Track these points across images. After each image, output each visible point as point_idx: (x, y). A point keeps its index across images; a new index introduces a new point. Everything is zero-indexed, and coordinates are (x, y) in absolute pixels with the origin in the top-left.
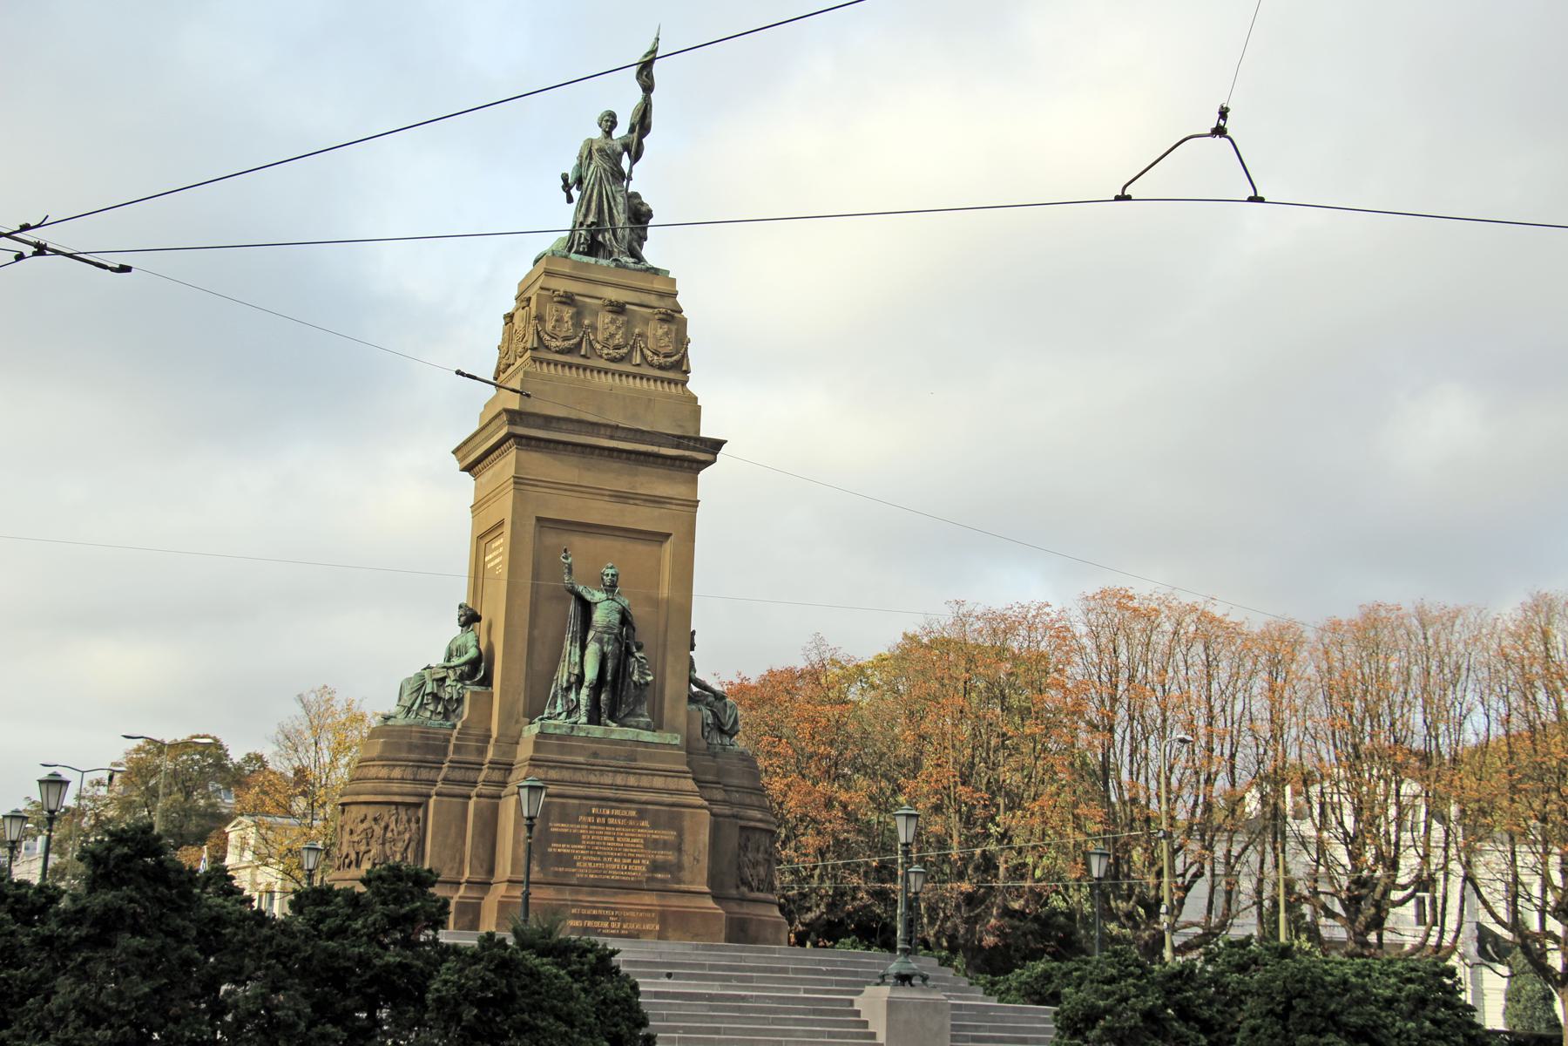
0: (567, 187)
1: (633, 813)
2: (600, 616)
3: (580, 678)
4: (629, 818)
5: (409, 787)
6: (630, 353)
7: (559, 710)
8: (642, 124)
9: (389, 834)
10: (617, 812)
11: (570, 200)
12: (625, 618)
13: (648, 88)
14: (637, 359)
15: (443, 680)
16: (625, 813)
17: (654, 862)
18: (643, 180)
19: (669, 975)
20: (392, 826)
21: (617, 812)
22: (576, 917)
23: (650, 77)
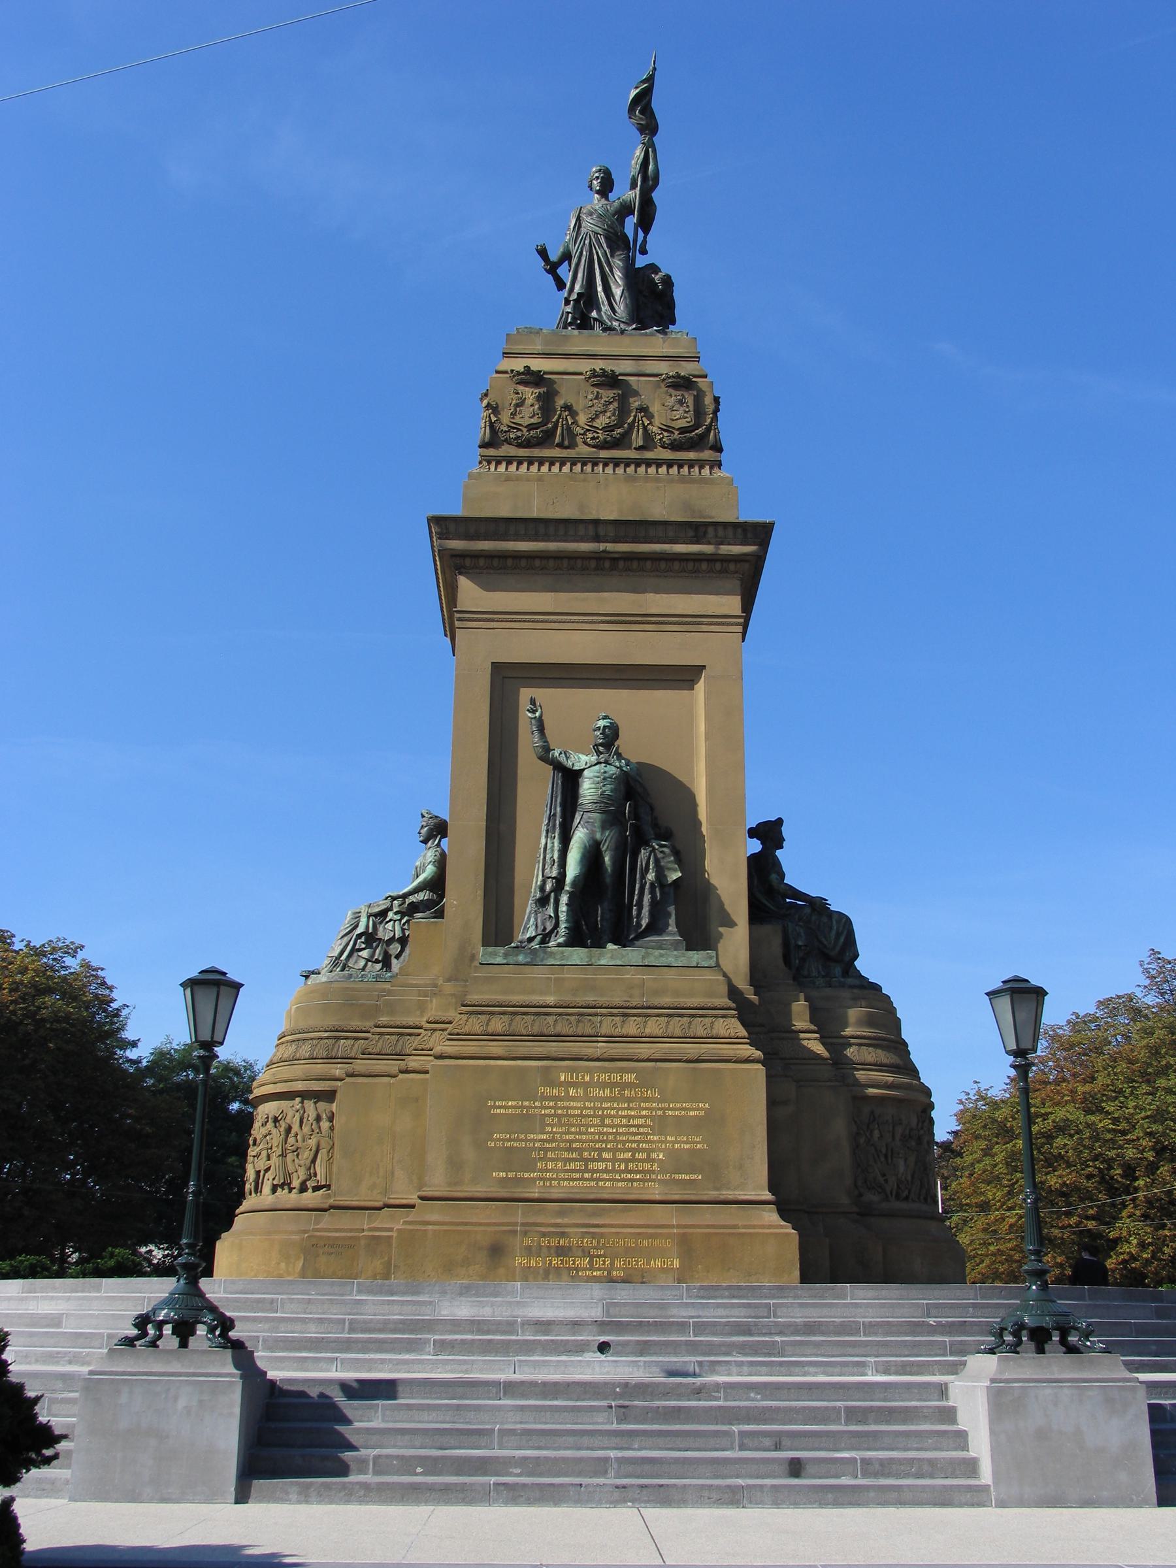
0: (552, 269)
1: (630, 1078)
2: (588, 789)
3: (560, 880)
4: (624, 1086)
5: (320, 1069)
6: (627, 434)
7: (531, 933)
8: (648, 180)
9: (291, 1140)
10: (604, 1077)
11: (560, 285)
13: (649, 127)
14: (637, 439)
16: (616, 1078)
17: (671, 1153)
18: (663, 250)
19: (603, 1347)
20: (296, 1128)
21: (604, 1077)
22: (529, 1251)
23: (648, 112)
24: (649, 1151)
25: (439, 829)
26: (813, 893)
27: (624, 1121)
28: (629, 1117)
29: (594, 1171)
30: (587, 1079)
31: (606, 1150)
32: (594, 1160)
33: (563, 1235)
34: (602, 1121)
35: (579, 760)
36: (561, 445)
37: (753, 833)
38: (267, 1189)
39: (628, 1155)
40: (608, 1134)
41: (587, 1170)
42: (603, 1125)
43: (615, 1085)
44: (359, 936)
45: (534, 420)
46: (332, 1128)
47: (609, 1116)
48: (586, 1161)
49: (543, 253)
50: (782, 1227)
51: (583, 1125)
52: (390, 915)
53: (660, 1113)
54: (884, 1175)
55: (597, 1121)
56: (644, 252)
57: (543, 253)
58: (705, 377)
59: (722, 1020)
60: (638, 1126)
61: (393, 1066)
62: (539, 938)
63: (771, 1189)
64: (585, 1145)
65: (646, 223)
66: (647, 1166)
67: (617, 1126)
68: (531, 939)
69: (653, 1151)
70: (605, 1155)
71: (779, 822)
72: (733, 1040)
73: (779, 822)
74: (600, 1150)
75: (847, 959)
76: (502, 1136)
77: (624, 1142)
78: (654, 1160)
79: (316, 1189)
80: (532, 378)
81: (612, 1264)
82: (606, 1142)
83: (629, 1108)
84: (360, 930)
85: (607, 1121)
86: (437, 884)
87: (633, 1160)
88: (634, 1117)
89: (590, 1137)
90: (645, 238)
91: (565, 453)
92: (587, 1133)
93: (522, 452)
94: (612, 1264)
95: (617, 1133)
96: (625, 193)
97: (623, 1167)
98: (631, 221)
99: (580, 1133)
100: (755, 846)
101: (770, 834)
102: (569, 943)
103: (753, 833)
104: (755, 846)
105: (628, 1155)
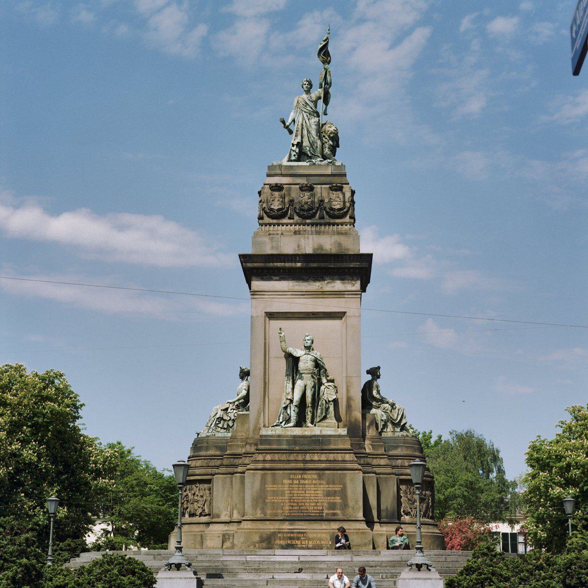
3: (291, 401)
7: (281, 421)
12: (318, 364)
15: (226, 409)
23: (327, 54)
24: (322, 502)
25: (244, 374)
29: (302, 510)
30: (300, 476)
31: (307, 502)
32: (302, 506)
33: (292, 533)
34: (305, 492)
35: (298, 352)
36: (289, 218)
37: (368, 372)
38: (187, 516)
41: (300, 510)
42: (305, 493)
43: (309, 479)
44: (218, 418)
45: (280, 207)
46: (210, 493)
48: (300, 506)
49: (283, 122)
50: (367, 529)
51: (298, 493)
52: (229, 410)
54: (411, 509)
55: (303, 492)
56: (325, 114)
57: (283, 122)
58: (348, 184)
59: (348, 454)
60: (318, 494)
61: (230, 470)
62: (284, 422)
63: (364, 516)
64: (300, 501)
65: (326, 101)
68: (281, 423)
70: (306, 504)
71: (379, 368)
72: (352, 462)
73: (379, 368)
74: (304, 503)
75: (402, 424)
76: (270, 498)
79: (205, 515)
80: (277, 188)
81: (308, 542)
82: (307, 499)
84: (218, 416)
86: (246, 398)
87: (316, 506)
88: (317, 490)
89: (301, 498)
90: (326, 107)
91: (291, 221)
92: (300, 496)
93: (275, 221)
94: (308, 542)
95: (310, 496)
96: (317, 92)
97: (312, 508)
98: (321, 102)
99: (298, 496)
100: (369, 377)
101: (374, 373)
102: (294, 426)
103: (368, 372)
104: (369, 377)
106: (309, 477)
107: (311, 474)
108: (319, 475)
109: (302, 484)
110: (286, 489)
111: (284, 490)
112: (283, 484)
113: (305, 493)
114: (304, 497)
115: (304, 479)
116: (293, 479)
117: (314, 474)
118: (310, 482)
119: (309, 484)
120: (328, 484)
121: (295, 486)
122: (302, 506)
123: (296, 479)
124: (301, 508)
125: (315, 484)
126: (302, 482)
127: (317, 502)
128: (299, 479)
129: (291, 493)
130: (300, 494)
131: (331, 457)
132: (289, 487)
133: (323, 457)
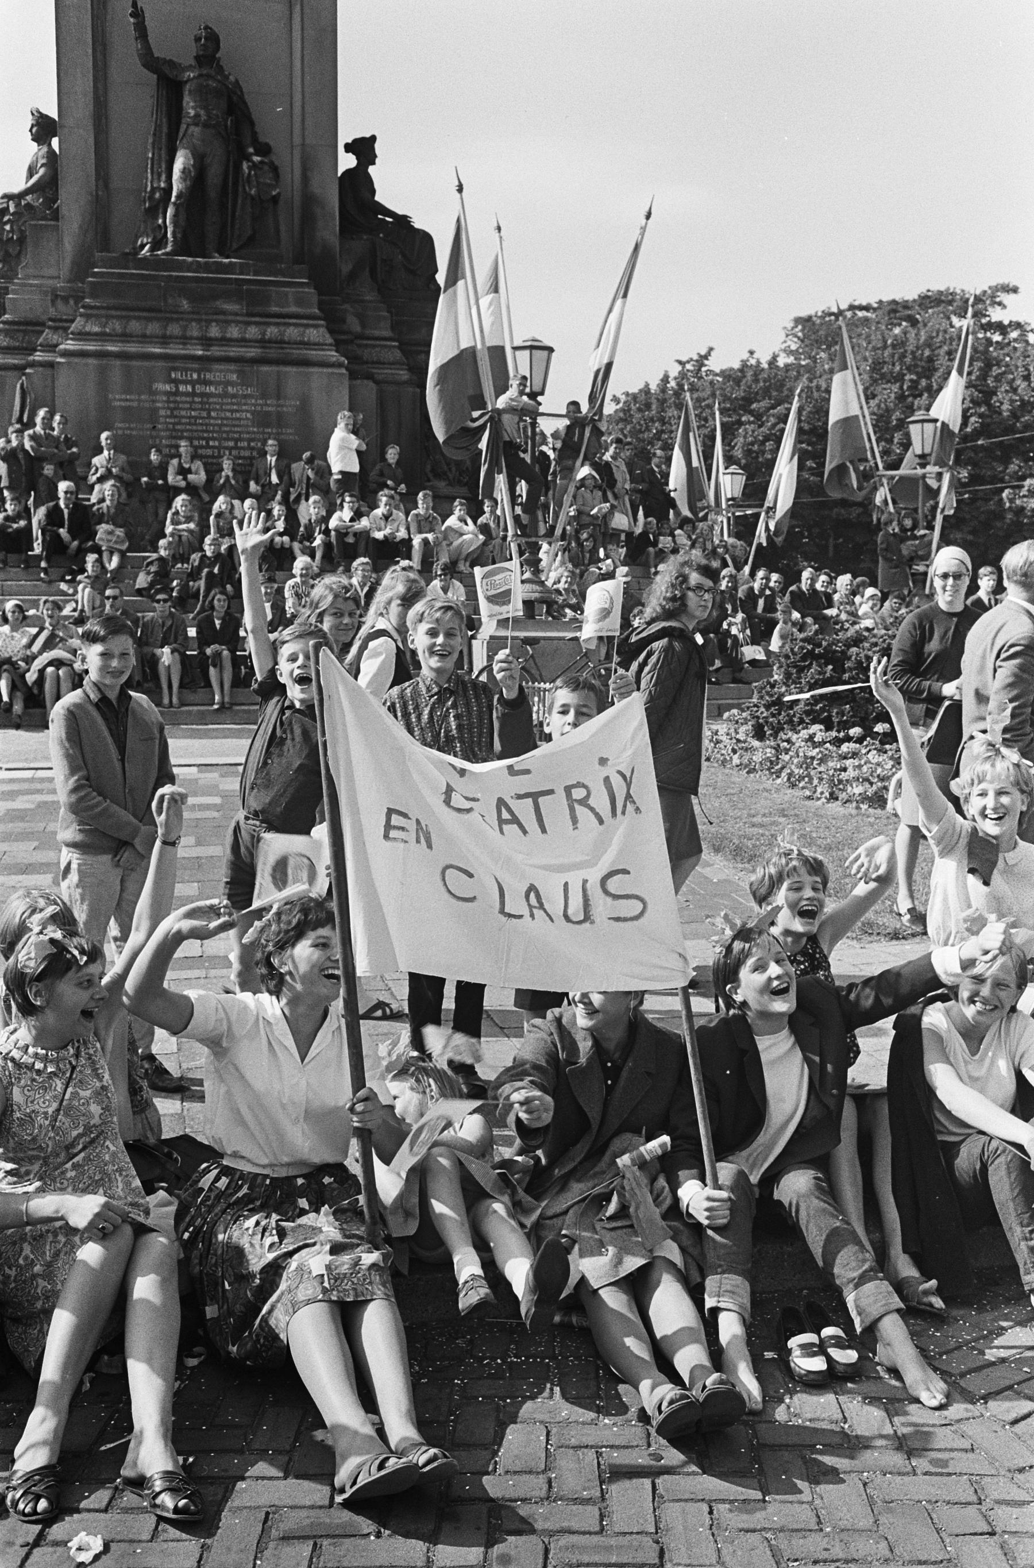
26: (400, 212)
27: (228, 414)
28: (232, 411)
30: (195, 376)
31: (214, 439)
32: (202, 447)
34: (209, 413)
37: (348, 148)
39: (231, 444)
40: (214, 425)
43: (219, 383)
47: (215, 410)
53: (259, 408)
55: (204, 414)
60: (239, 419)
66: (247, 453)
67: (222, 419)
69: (253, 440)
71: (373, 138)
73: (373, 138)
74: (207, 440)
77: (227, 432)
78: (253, 449)
82: (213, 432)
83: (233, 404)
85: (213, 414)
88: (237, 411)
95: (222, 425)
101: (364, 149)
103: (348, 148)
105: (231, 444)
106: (219, 376)
107: (221, 371)
108: (241, 373)
109: (203, 395)
110: (159, 405)
111: (157, 409)
112: (153, 393)
113: (209, 417)
114: (206, 425)
115: (206, 383)
116: (176, 382)
117: (232, 372)
118: (220, 389)
119: (219, 396)
120: (264, 396)
121: (184, 399)
122: (202, 447)
123: (185, 382)
124: (200, 451)
125: (234, 396)
126: (199, 389)
127: (240, 439)
128: (193, 383)
129: (172, 416)
130: (196, 418)
131: (272, 332)
132: (168, 402)
133: (253, 332)
